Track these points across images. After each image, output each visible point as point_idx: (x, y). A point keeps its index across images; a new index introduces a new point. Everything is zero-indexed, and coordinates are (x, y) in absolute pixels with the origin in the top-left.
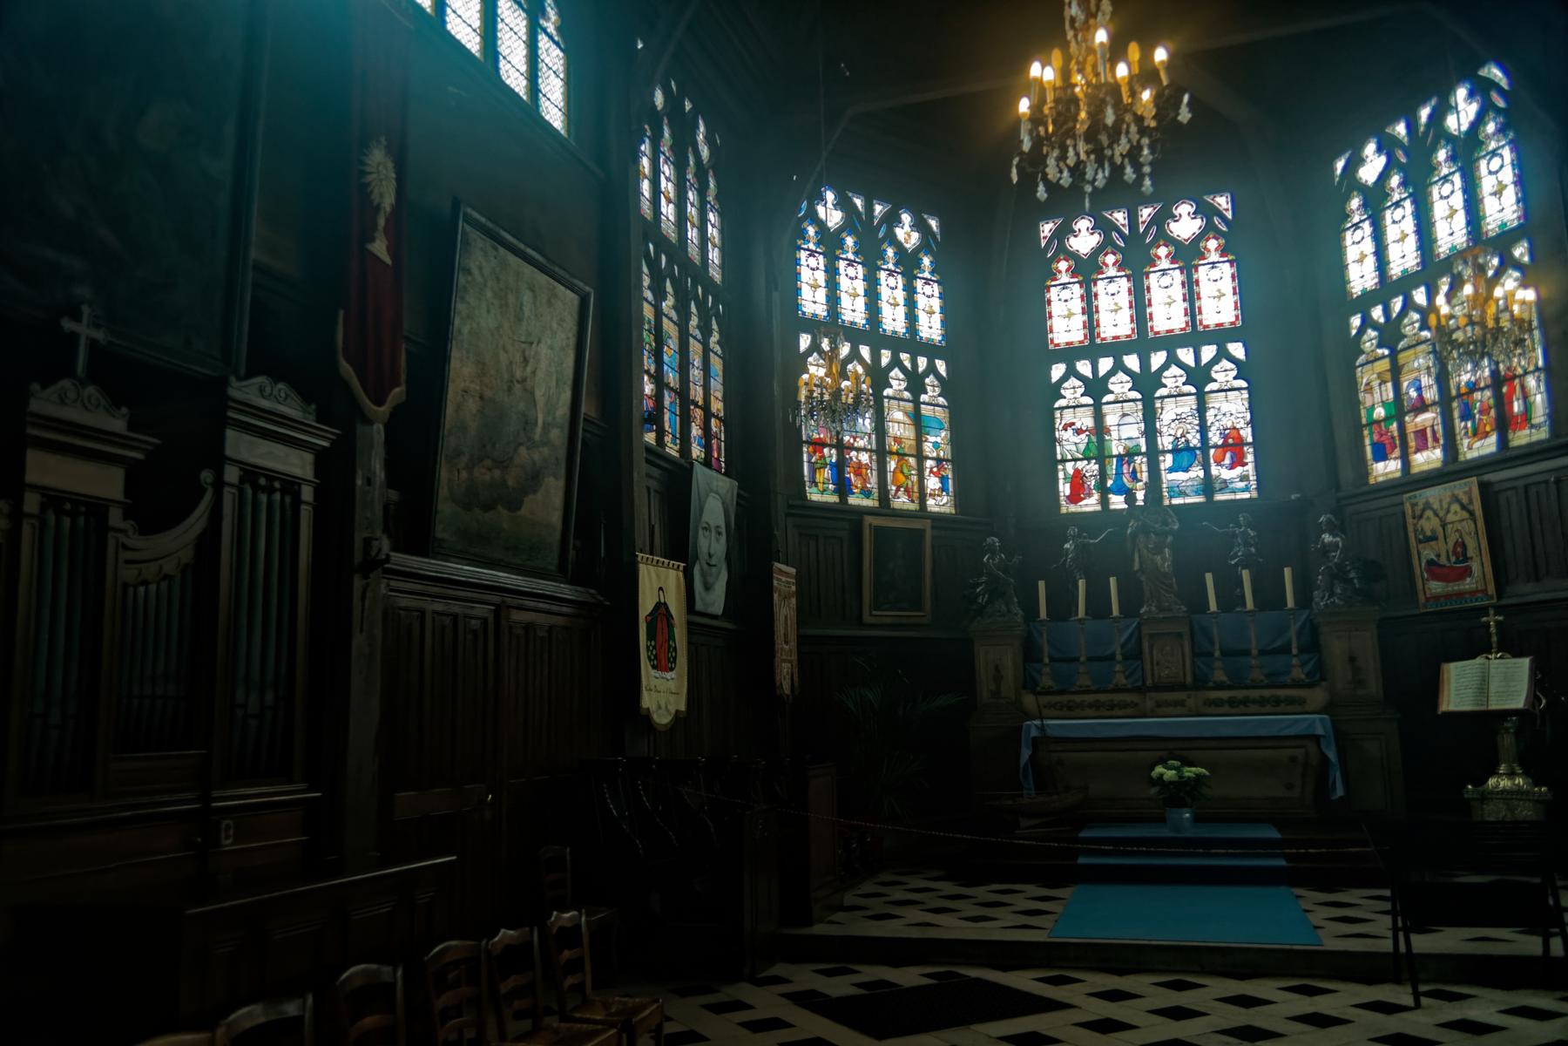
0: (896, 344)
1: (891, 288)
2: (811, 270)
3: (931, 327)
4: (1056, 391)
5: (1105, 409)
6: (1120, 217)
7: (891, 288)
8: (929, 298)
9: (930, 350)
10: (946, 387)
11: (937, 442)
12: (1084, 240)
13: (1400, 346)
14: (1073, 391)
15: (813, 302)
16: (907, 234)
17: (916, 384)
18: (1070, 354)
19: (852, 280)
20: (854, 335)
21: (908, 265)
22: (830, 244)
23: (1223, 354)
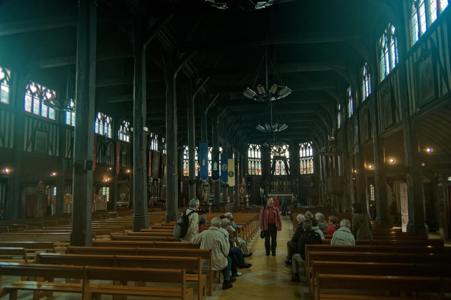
0: (256, 159)
1: (256, 153)
2: (249, 152)
3: (260, 157)
7: (256, 153)
8: (259, 153)
9: (259, 159)
10: (261, 162)
11: (260, 168)
15: (249, 156)
16: (258, 147)
17: (258, 162)
19: (253, 152)
20: (253, 158)
21: (258, 150)
22: (251, 150)
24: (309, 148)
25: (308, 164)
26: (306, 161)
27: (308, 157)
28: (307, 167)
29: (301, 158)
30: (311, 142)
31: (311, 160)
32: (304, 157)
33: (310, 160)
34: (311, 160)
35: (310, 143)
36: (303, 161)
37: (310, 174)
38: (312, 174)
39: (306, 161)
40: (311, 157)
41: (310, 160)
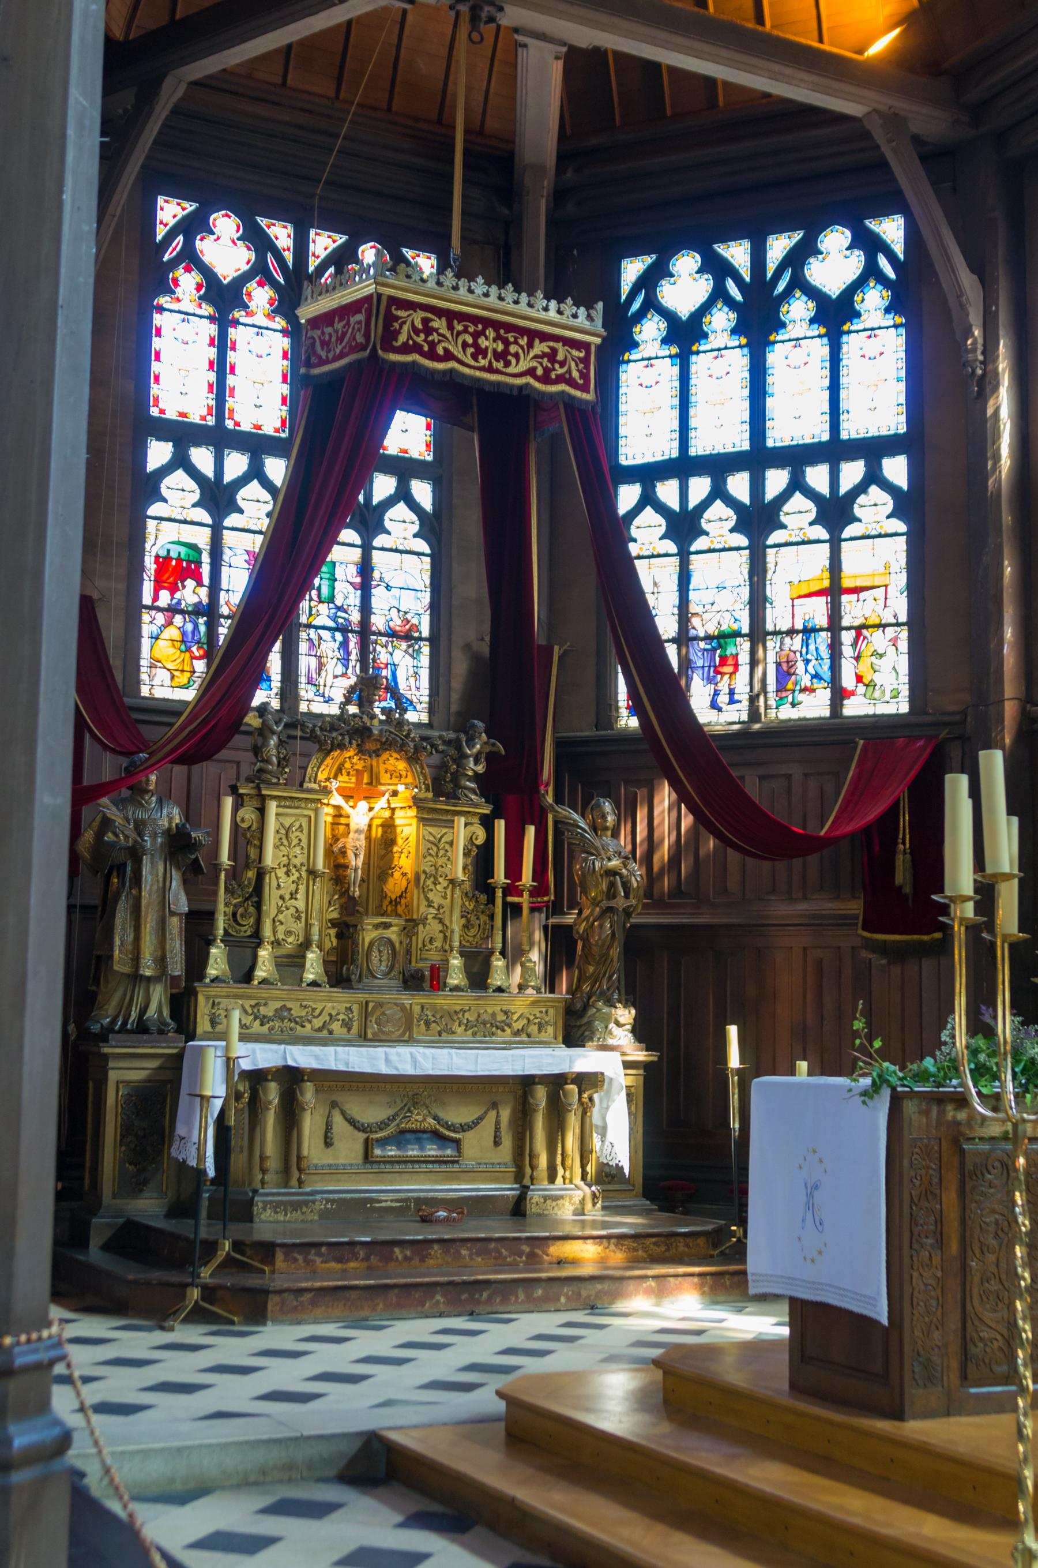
4: (149, 487)
5: (229, 538)
6: (282, 234)
12: (225, 250)
13: (695, 547)
14: (179, 493)
18: (183, 435)
23: (403, 495)
24: (835, 315)
25: (797, 563)
26: (758, 521)
27: (796, 458)
28: (791, 617)
29: (648, 475)
30: (892, 230)
31: (875, 509)
32: (718, 467)
33: (835, 513)
34: (875, 509)
35: (869, 244)
36: (684, 527)
37: (834, 736)
38: (878, 730)
39: (758, 521)
40: (873, 450)
41: (835, 513)
